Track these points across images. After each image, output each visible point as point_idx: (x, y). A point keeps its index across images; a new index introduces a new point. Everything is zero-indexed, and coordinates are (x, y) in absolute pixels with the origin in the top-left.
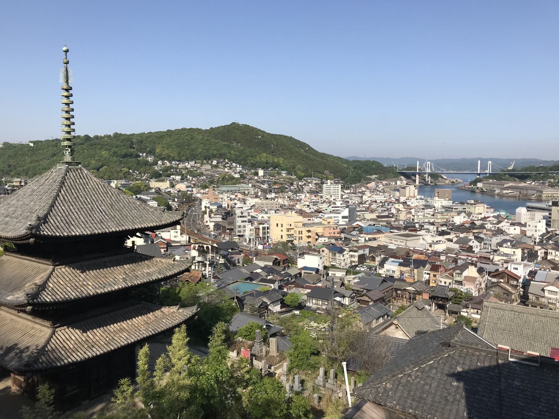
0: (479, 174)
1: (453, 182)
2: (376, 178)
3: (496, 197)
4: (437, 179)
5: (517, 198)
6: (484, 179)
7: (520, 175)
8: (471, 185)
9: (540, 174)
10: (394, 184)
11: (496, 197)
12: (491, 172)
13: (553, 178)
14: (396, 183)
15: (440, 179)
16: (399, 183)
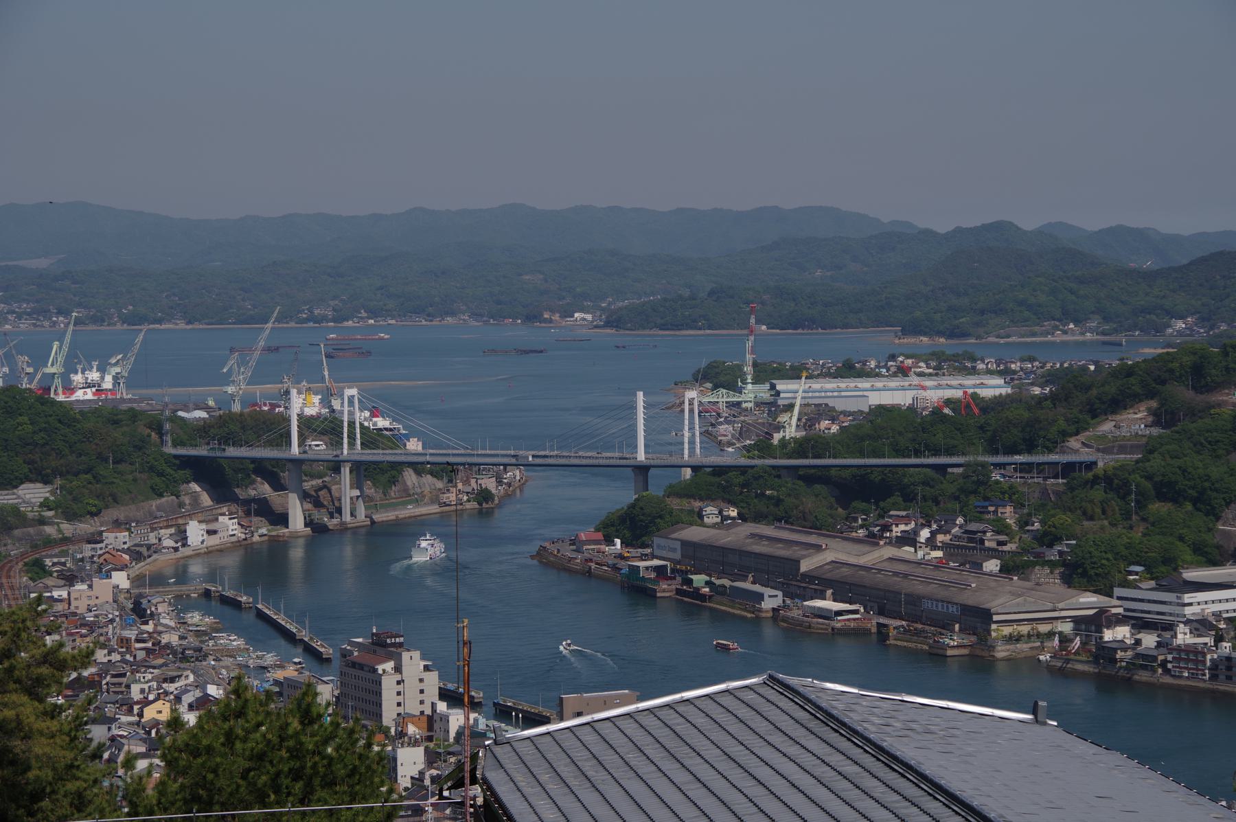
0: (642, 470)
1: (484, 496)
2: (45, 505)
3: (769, 631)
4: (393, 481)
5: (874, 637)
6: (675, 503)
7: (846, 474)
8: (609, 541)
9: (942, 469)
10: (168, 543)
11: (769, 631)
12: (700, 457)
13: (1010, 495)
14: (182, 536)
15: (410, 477)
16: (195, 532)
